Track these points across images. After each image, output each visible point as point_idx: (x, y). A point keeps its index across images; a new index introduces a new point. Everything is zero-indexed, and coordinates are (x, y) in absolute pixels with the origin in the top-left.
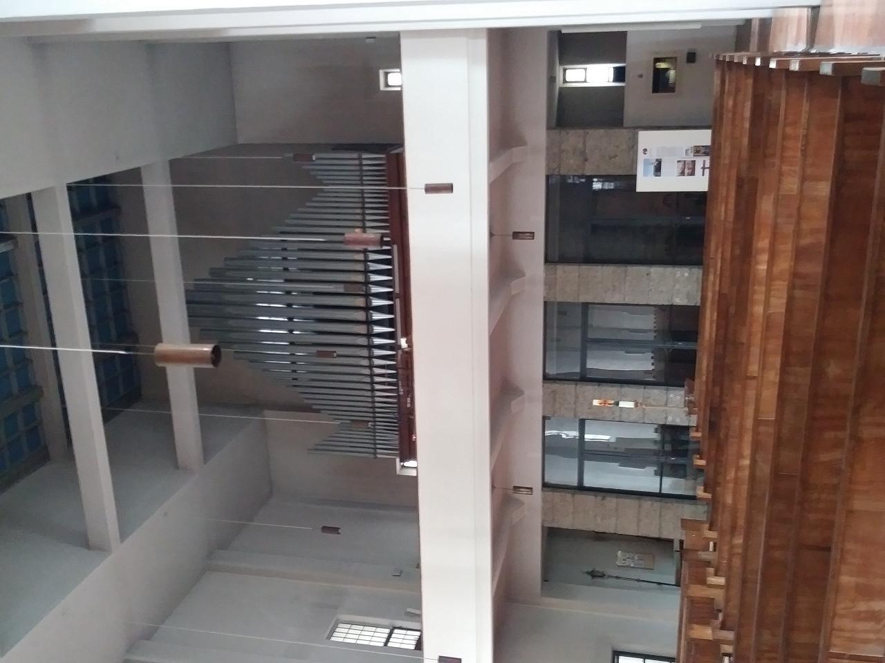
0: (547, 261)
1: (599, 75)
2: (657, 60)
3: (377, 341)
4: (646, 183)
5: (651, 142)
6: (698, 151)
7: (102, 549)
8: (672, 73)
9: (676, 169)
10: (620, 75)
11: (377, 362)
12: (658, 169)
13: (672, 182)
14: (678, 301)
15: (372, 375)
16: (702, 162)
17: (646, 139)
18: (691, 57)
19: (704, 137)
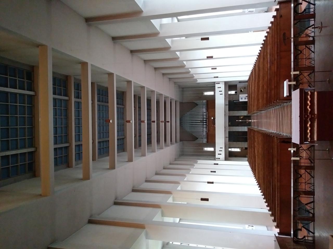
0: (229, 111)
1: (233, 92)
2: (241, 89)
3: (204, 125)
4: (241, 100)
5: (241, 96)
6: (246, 97)
7: (173, 144)
8: (243, 90)
9: (244, 99)
10: (236, 92)
11: (204, 128)
12: (242, 99)
13: (244, 100)
14: (245, 115)
15: (203, 130)
16: (247, 98)
17: (240, 95)
18: (245, 88)
19: (247, 95)
